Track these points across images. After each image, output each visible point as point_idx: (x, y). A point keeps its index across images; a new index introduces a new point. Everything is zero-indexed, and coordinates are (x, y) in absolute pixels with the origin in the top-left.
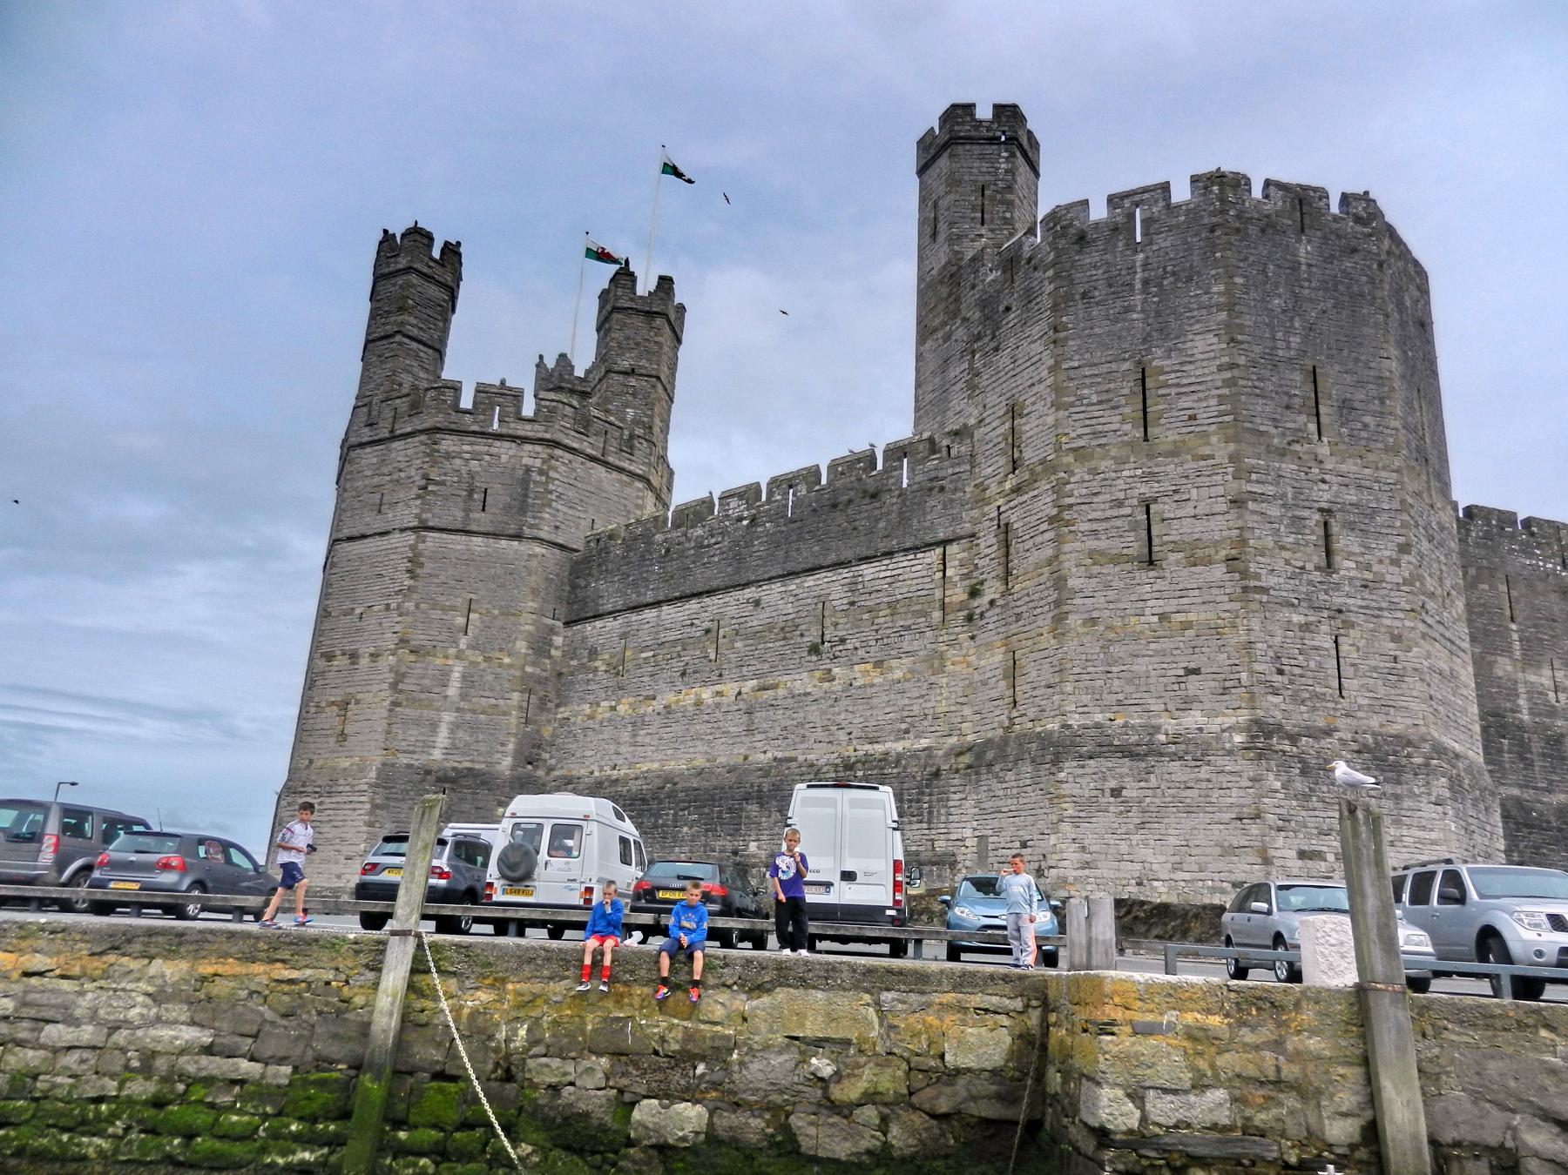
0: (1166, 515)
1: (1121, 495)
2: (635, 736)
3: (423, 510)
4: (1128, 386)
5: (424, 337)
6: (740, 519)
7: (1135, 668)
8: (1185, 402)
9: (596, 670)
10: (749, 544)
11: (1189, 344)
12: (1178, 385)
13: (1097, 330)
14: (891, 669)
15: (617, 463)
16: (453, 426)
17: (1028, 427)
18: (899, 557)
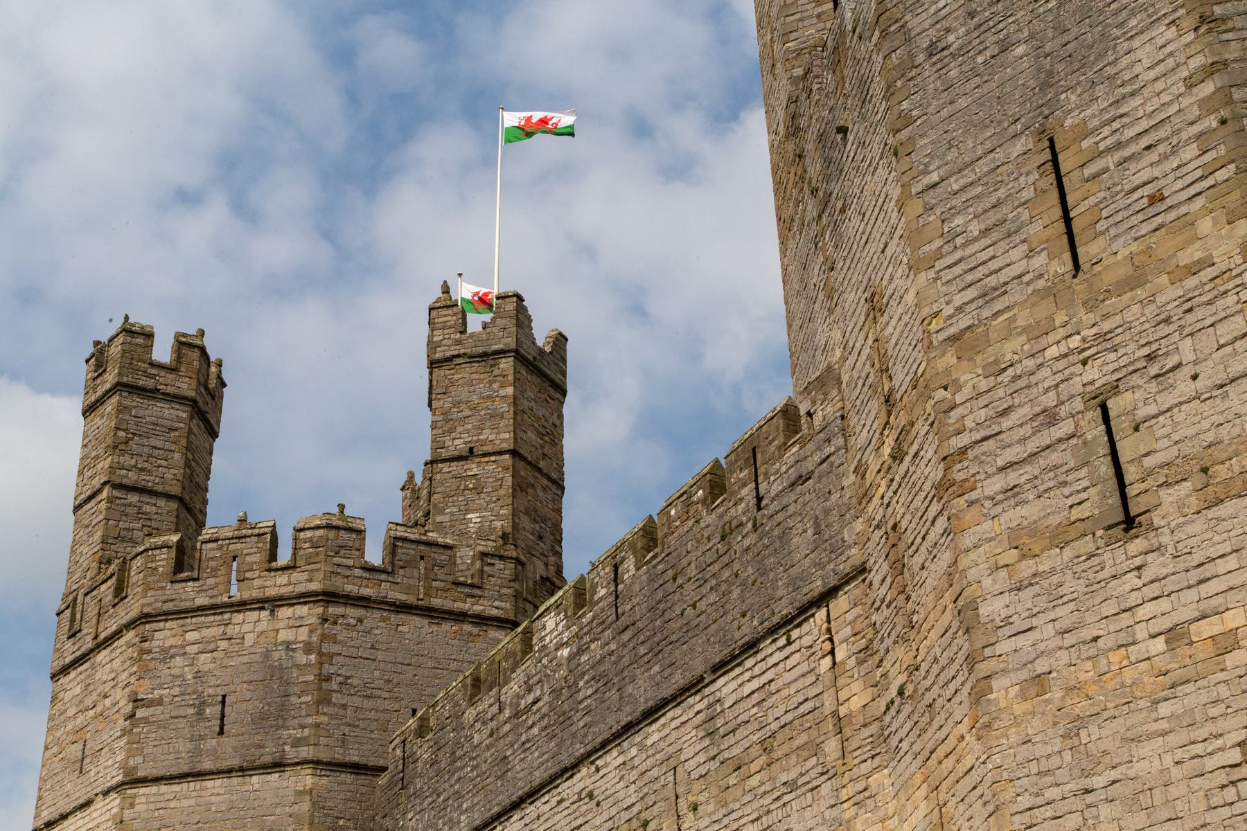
0: (1142, 413)
1: (1049, 400)
3: (130, 754)
4: (1031, 181)
5: (150, 481)
7: (1139, 768)
8: (1141, 172)
11: (1125, 61)
12: (1119, 145)
13: (962, 102)
15: (449, 605)
16: (169, 606)
18: (767, 647)
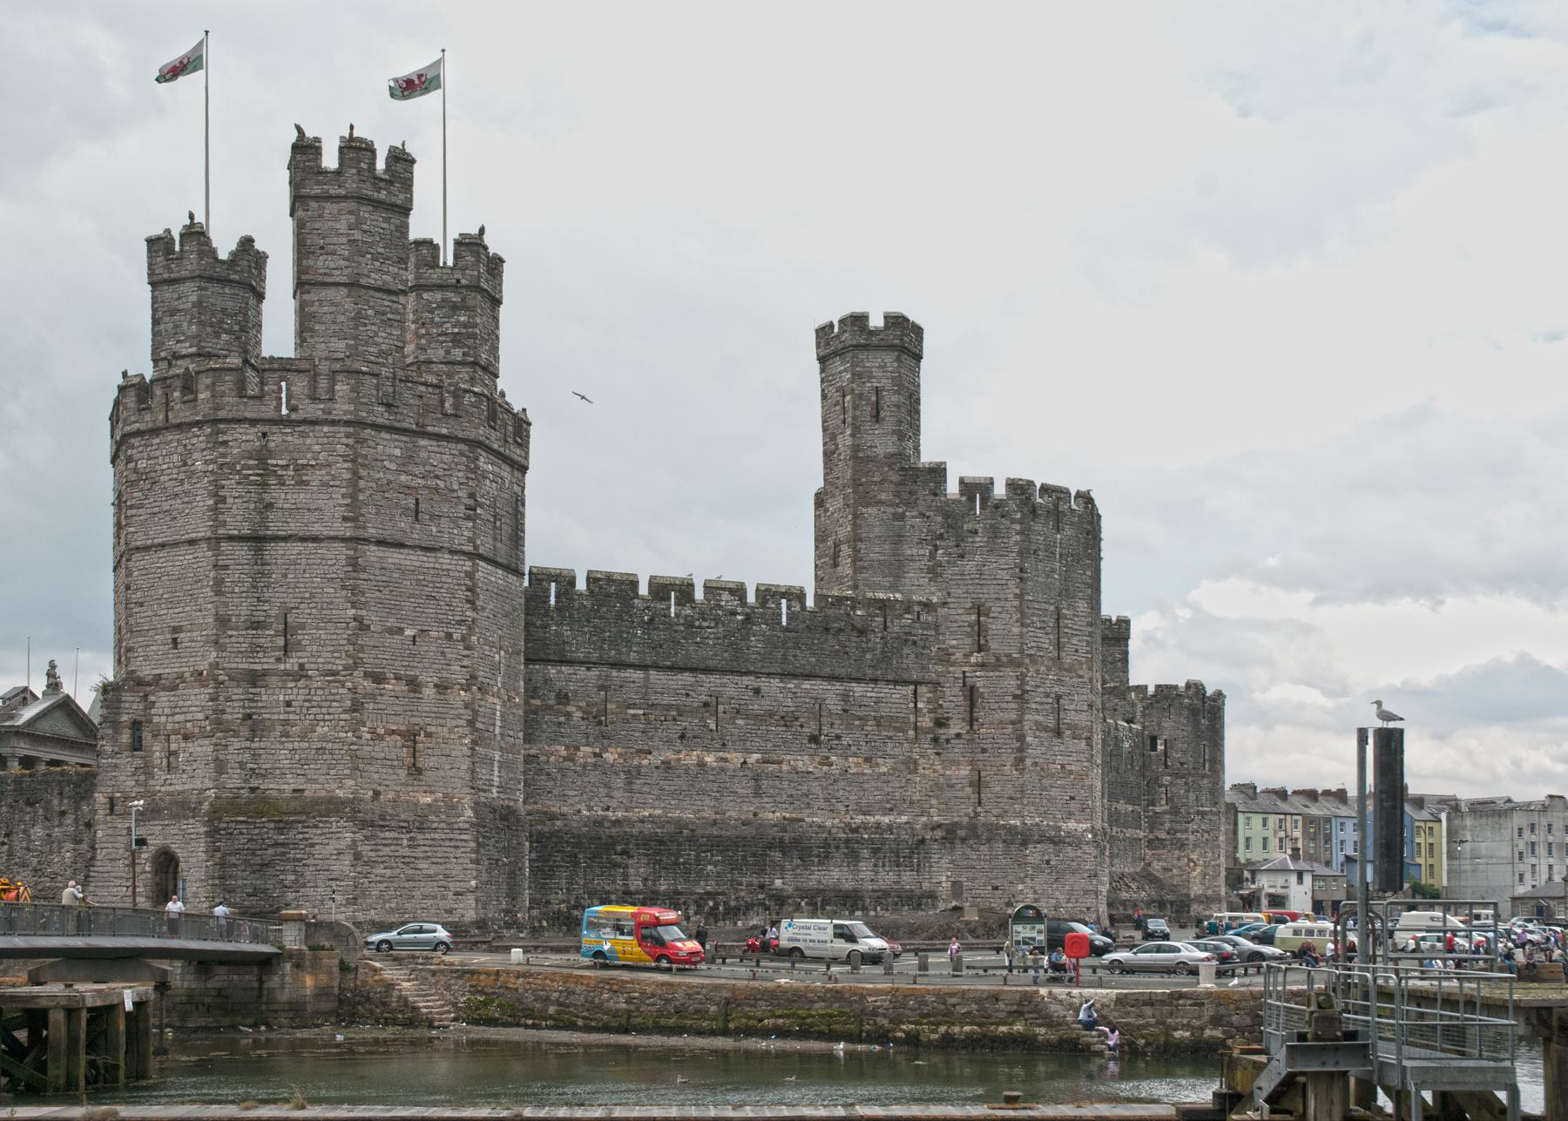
2: (630, 783)
6: (734, 613)
9: (569, 715)
10: (746, 638)
14: (878, 765)
17: (994, 627)
